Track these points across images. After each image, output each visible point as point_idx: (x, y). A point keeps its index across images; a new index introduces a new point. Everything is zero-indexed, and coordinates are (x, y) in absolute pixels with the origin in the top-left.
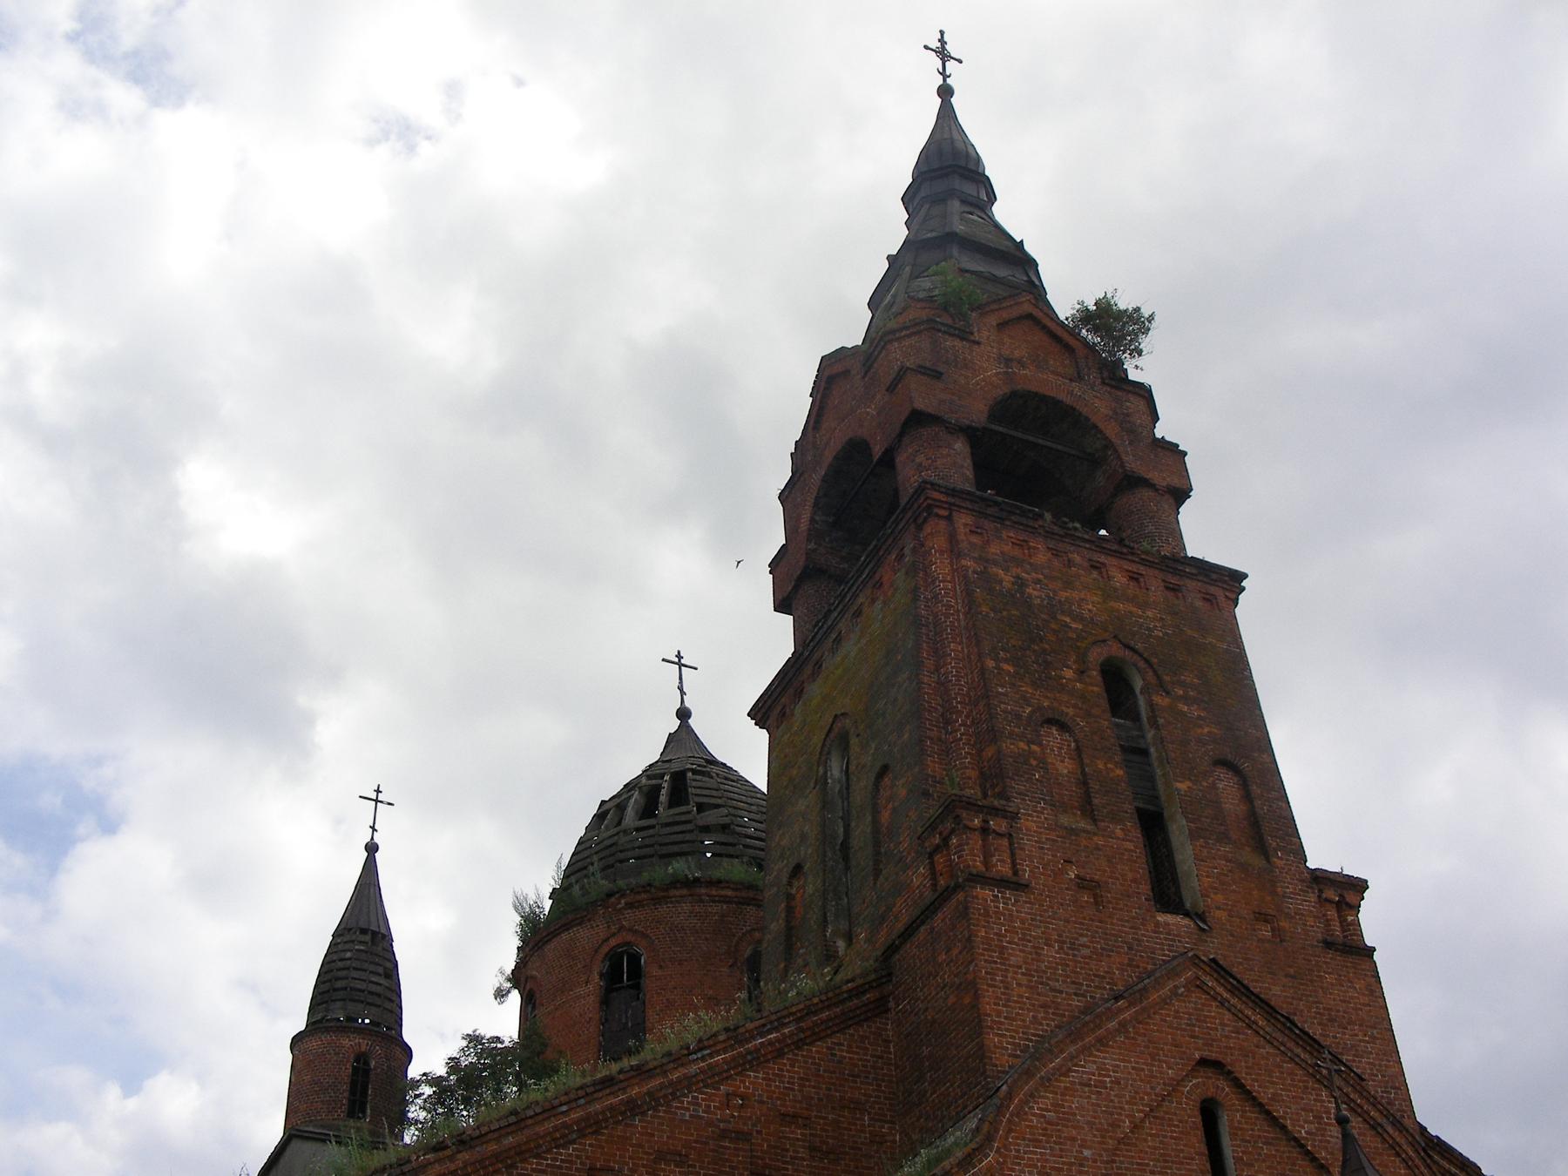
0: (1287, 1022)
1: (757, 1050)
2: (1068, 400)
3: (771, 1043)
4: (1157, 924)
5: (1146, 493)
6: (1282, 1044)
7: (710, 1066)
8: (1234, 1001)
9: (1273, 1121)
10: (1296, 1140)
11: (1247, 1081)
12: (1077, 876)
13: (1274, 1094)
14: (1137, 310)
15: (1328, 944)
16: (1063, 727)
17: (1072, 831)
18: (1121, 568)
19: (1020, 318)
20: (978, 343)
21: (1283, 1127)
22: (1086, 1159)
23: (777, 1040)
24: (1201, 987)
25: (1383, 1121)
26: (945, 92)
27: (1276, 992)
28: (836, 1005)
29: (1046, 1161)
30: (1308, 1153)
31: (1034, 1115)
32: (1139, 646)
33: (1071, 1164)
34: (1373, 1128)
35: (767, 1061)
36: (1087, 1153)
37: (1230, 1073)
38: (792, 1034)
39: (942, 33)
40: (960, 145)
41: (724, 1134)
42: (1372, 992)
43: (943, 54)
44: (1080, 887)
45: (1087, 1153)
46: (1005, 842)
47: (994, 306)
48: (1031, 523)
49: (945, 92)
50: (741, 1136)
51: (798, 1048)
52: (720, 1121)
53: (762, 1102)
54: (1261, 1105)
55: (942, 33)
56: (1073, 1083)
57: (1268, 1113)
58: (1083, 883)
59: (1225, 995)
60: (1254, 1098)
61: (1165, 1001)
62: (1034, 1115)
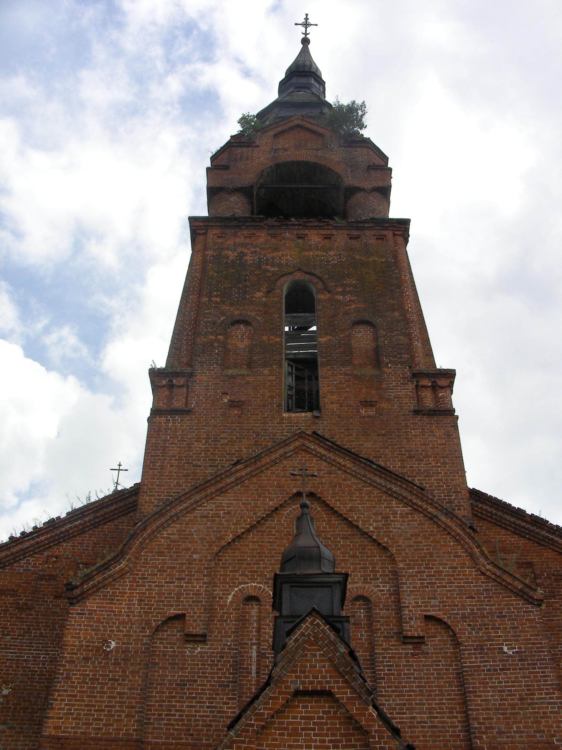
0: (368, 463)
1: (67, 531)
2: (312, 159)
3: (76, 526)
4: (282, 419)
5: (359, 195)
6: (364, 476)
7: (37, 543)
8: (331, 455)
9: (350, 524)
10: (366, 533)
11: (332, 502)
12: (229, 401)
13: (351, 507)
14: (354, 103)
15: (416, 412)
16: (246, 323)
17: (233, 377)
18: (318, 234)
19: (291, 128)
20: (258, 146)
21: (357, 527)
22: (195, 560)
23: (81, 524)
24: (307, 451)
25: (439, 514)
26: (305, 41)
27: (367, 447)
28: (121, 500)
29: (165, 563)
30: (375, 540)
31: (164, 538)
32: (317, 272)
33: (183, 564)
34: (431, 519)
35: (75, 536)
36: (195, 556)
37: (320, 498)
38: (90, 521)
39: (307, 15)
40: (308, 63)
41: (42, 578)
42: (449, 436)
43: (306, 24)
44: (230, 406)
45: (195, 556)
46: (184, 390)
47: (274, 126)
48: (258, 224)
49: (305, 41)
50: (52, 577)
51: (95, 527)
52: (41, 571)
53: (68, 558)
54: (341, 515)
55: (307, 15)
56: (196, 517)
57: (346, 519)
58: (233, 404)
59: (323, 452)
60: (336, 512)
61: (275, 463)
62: (164, 538)
